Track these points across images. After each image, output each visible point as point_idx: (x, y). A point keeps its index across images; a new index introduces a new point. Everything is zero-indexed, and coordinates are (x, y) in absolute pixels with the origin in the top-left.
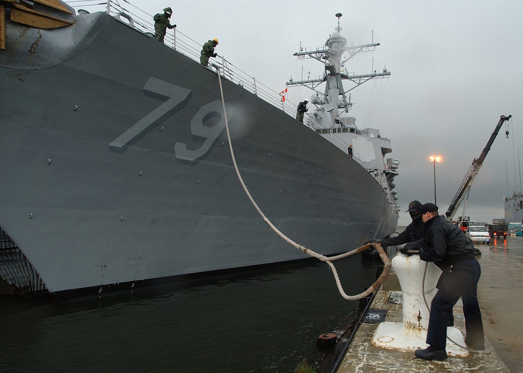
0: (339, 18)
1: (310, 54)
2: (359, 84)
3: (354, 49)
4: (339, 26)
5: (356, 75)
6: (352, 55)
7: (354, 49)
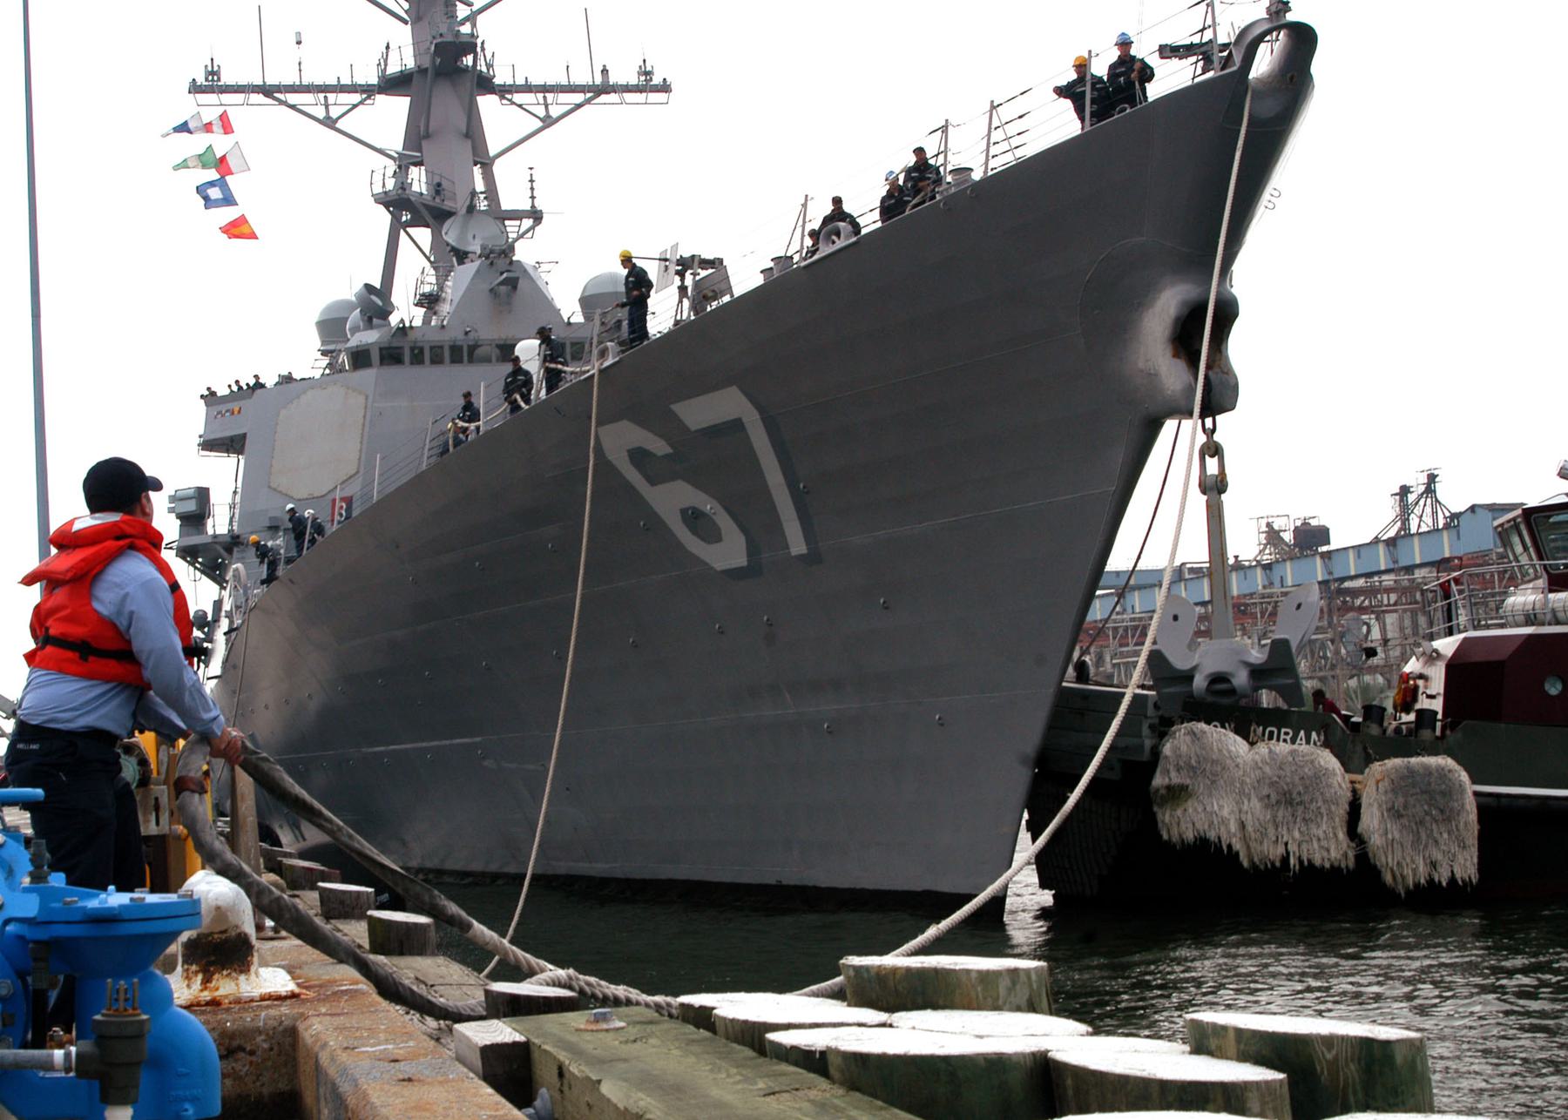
2: (548, 122)
5: (520, 81)
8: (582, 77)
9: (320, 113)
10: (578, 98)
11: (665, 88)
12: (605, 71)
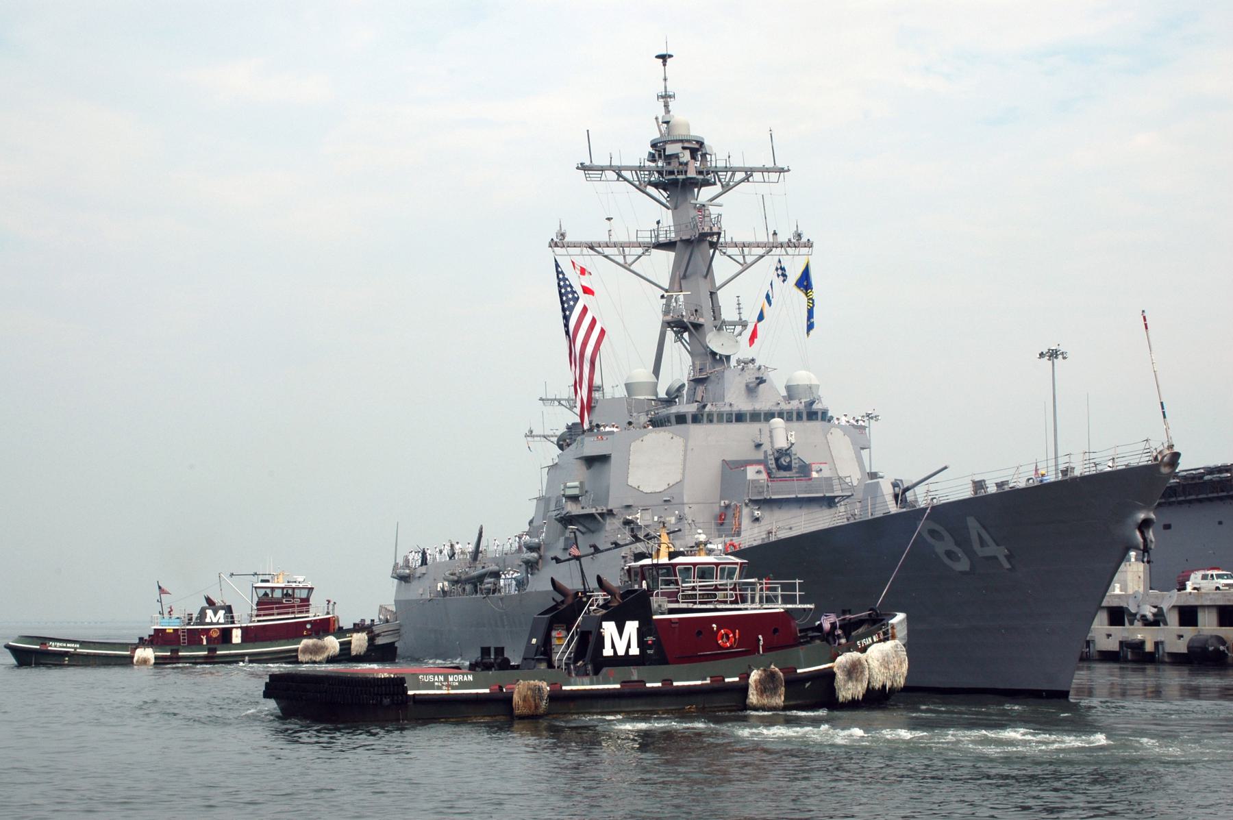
0: (664, 65)
1: (618, 171)
2: (746, 267)
3: (729, 174)
4: (666, 87)
6: (727, 188)
7: (729, 174)
8: (762, 238)
9: (620, 259)
10: (761, 251)
11: (809, 244)
12: (775, 234)
